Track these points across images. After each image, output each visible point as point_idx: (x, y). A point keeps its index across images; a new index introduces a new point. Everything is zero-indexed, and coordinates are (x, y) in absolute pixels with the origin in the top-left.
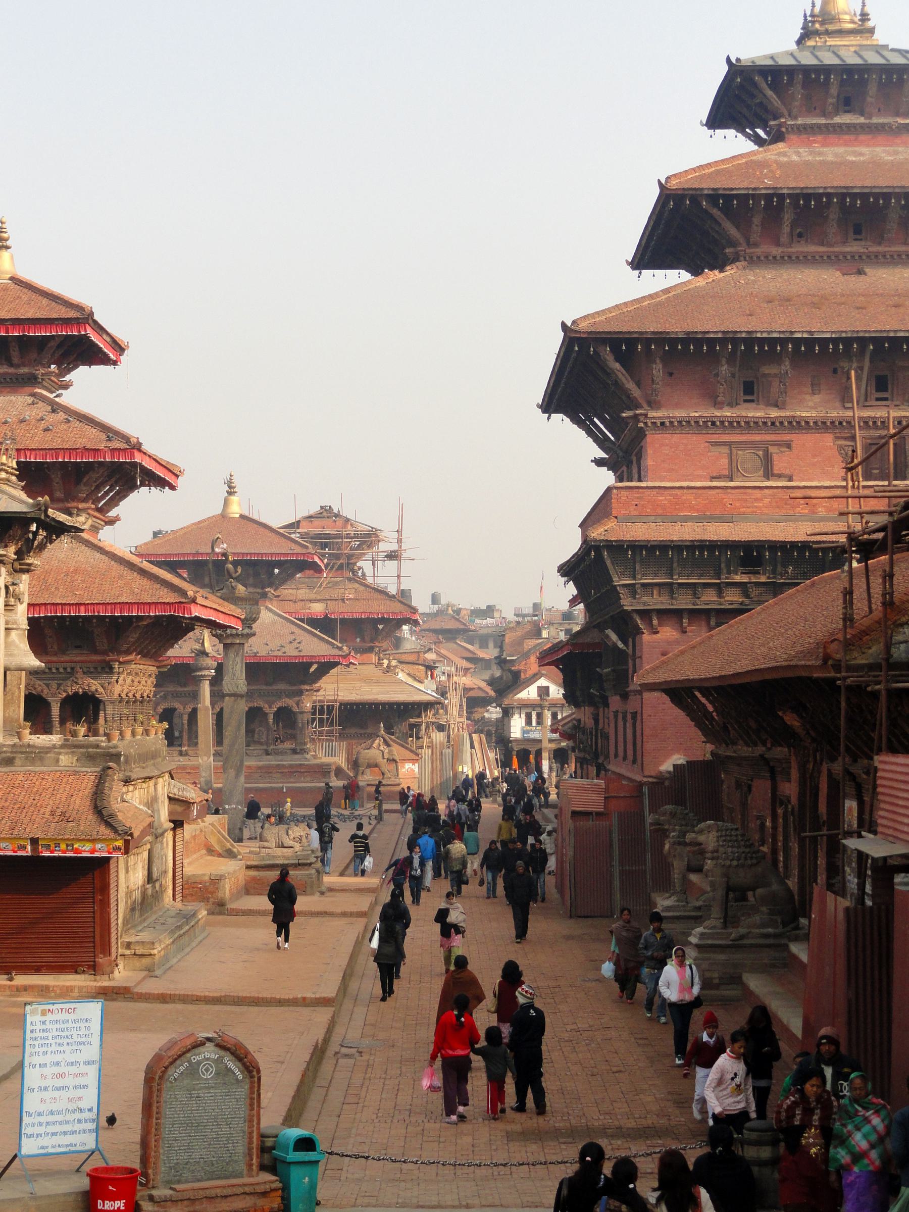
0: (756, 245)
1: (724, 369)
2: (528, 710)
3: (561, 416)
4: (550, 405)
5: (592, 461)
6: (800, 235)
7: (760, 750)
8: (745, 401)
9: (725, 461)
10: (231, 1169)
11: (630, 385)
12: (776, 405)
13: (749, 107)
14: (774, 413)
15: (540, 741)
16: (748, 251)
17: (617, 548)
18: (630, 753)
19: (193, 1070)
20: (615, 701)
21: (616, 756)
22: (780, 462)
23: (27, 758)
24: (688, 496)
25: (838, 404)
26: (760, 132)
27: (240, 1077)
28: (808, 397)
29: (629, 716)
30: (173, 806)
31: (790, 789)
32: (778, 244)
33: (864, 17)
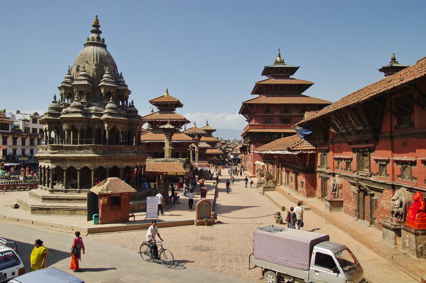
1: (264, 108)
3: (241, 114)
9: (264, 121)
14: (271, 115)
18: (251, 161)
19: (203, 204)
20: (248, 153)
22: (272, 121)
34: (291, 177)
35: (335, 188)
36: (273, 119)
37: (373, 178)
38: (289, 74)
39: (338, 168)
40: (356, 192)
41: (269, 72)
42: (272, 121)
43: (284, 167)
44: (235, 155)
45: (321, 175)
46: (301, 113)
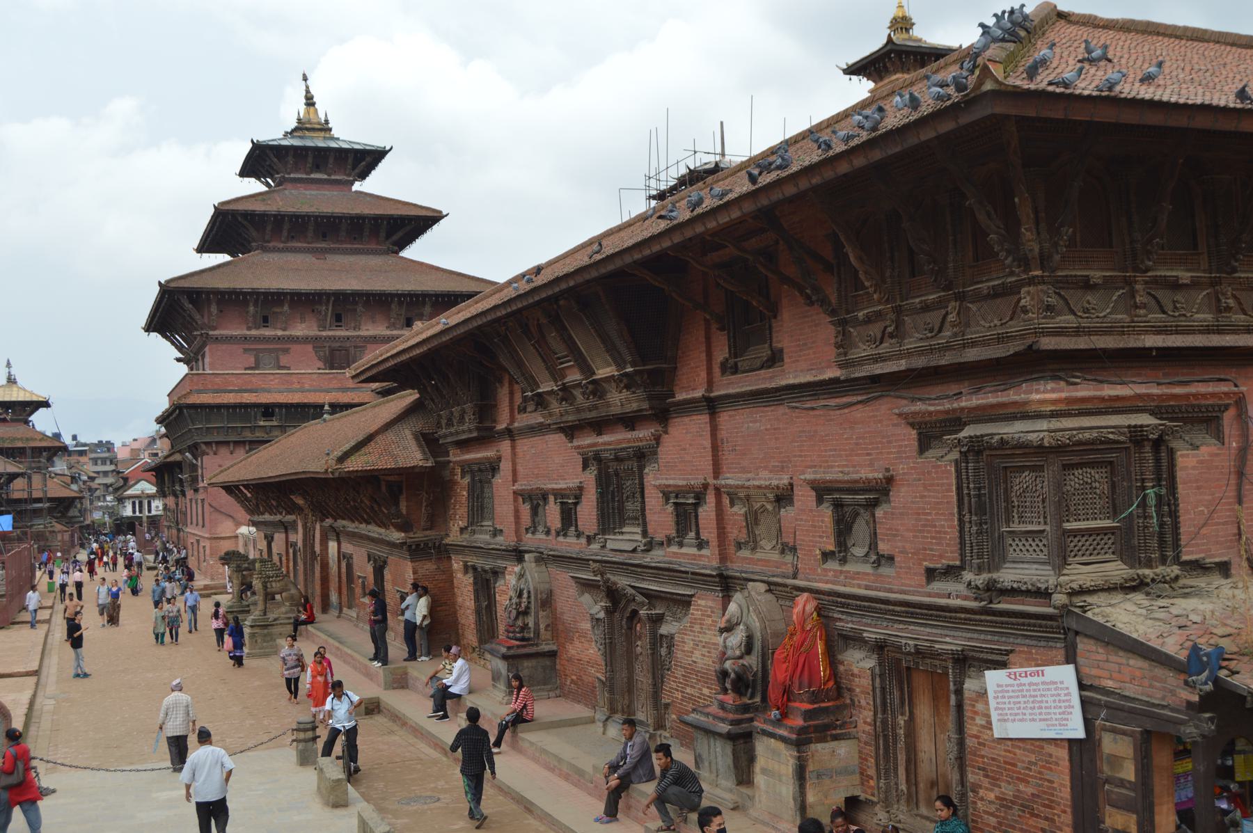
0: (269, 242)
1: (251, 309)
2: (131, 501)
3: (156, 334)
4: (149, 328)
6: (293, 237)
7: (278, 517)
9: (251, 360)
11: (197, 317)
13: (263, 167)
14: (280, 333)
20: (190, 493)
24: (233, 379)
25: (316, 328)
26: (269, 180)
29: (199, 501)
31: (298, 537)
33: (327, 122)
34: (359, 577)
35: (523, 605)
36: (286, 351)
37: (657, 557)
38: (349, 175)
39: (533, 529)
40: (602, 615)
41: (270, 166)
42: (284, 360)
43: (333, 540)
44: (134, 504)
45: (473, 560)
46: (399, 329)
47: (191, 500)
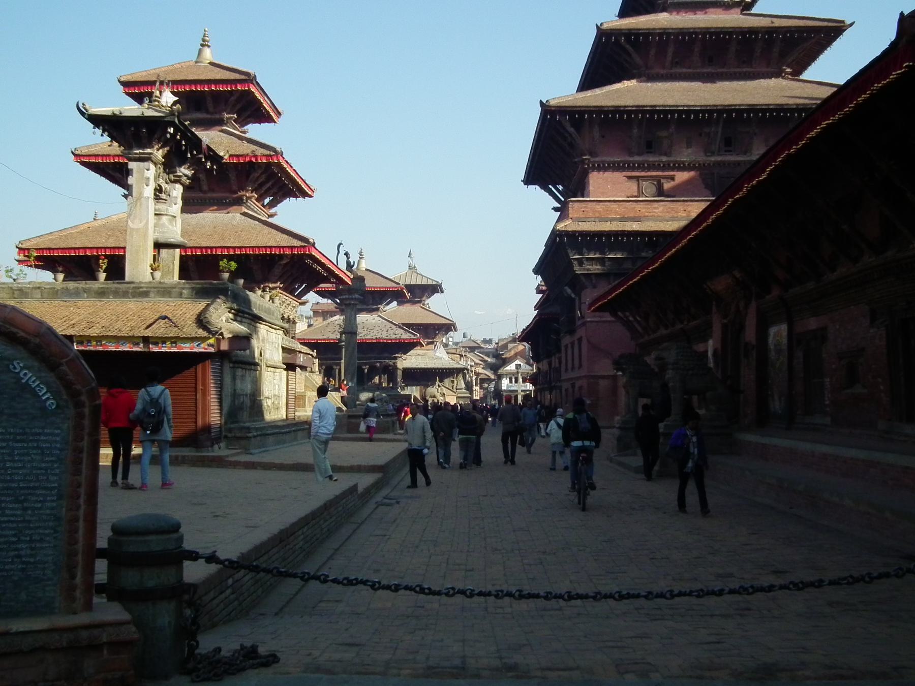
1: (635, 131)
3: (534, 186)
5: (552, 209)
6: (677, 63)
8: (648, 152)
9: (636, 188)
10: (23, 596)
12: (666, 154)
15: (517, 391)
16: (647, 72)
17: (572, 236)
21: (567, 370)
23: (158, 292)
27: (51, 404)
28: (684, 149)
29: (576, 343)
30: (285, 354)
32: (664, 68)
47: (566, 346)
